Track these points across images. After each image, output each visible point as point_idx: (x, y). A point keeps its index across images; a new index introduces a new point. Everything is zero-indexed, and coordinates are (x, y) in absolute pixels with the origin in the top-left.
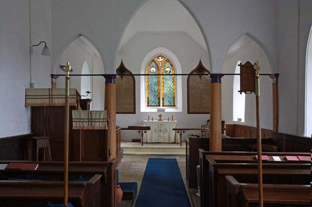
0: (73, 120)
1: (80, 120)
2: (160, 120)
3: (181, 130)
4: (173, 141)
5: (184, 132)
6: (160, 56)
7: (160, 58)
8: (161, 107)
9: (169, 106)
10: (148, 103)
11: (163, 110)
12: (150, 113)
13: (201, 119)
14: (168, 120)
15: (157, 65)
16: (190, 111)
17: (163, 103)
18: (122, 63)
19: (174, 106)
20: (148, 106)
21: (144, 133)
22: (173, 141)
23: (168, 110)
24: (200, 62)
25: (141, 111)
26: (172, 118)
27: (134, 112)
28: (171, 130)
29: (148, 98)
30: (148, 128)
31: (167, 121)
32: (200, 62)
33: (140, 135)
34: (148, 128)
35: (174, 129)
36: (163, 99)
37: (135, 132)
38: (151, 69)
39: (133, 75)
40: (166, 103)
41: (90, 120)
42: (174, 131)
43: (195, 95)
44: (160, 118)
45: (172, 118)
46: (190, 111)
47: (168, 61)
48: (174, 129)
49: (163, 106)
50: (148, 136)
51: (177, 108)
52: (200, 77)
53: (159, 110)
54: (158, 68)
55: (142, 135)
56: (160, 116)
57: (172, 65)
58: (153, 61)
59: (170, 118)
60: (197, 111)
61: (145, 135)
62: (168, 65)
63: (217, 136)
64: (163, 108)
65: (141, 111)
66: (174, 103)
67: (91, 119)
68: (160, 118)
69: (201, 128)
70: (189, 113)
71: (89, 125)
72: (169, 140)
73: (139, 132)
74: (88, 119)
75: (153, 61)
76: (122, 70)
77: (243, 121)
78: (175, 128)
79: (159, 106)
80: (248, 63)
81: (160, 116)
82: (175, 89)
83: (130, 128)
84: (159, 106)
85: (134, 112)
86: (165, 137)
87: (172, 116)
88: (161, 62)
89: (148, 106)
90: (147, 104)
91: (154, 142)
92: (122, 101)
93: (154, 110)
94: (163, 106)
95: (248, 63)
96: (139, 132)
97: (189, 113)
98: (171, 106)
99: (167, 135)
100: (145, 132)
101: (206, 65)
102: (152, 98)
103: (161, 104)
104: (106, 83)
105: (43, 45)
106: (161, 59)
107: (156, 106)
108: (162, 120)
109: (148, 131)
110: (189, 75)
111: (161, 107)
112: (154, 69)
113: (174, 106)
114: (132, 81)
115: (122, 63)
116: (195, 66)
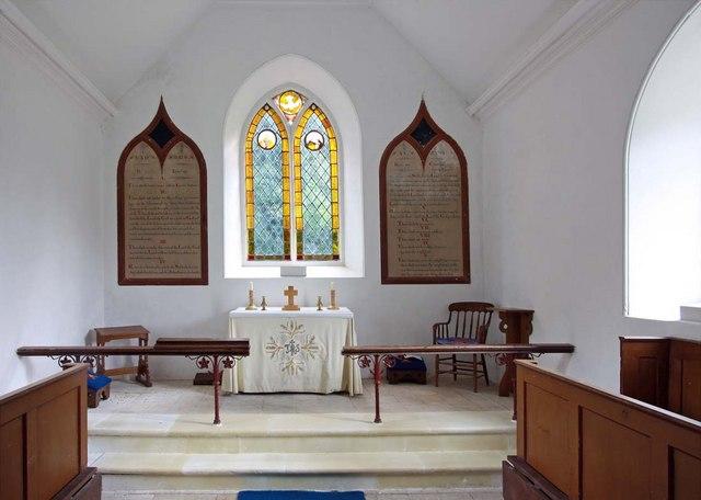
2: (291, 306)
4: (339, 388)
7: (289, 98)
9: (318, 258)
11: (301, 273)
13: (432, 301)
14: (320, 304)
15: (280, 123)
17: (300, 248)
18: (162, 108)
19: (336, 257)
20: (251, 258)
21: (221, 365)
22: (336, 384)
23: (316, 270)
24: (423, 107)
25: (226, 276)
26: (333, 297)
27: (204, 281)
29: (251, 232)
30: (242, 348)
31: (313, 310)
32: (423, 107)
34: (242, 348)
43: (404, 220)
44: (291, 300)
45: (333, 297)
47: (314, 108)
50: (242, 372)
52: (424, 156)
53: (285, 273)
54: (283, 131)
56: (291, 292)
57: (327, 124)
58: (267, 108)
59: (327, 298)
62: (316, 121)
64: (302, 263)
65: (226, 276)
68: (291, 300)
70: (386, 280)
72: (259, 385)
76: (162, 133)
79: (288, 258)
81: (291, 292)
84: (288, 258)
85: (204, 281)
86: (306, 372)
87: (332, 294)
89: (251, 258)
91: (270, 391)
92: (163, 242)
93: (270, 271)
97: (386, 280)
98: (326, 258)
99: (314, 365)
101: (439, 118)
103: (294, 253)
106: (290, 104)
107: (279, 258)
108: (296, 308)
111: (294, 262)
113: (336, 257)
114: (195, 172)
115: (162, 107)
116: (406, 120)
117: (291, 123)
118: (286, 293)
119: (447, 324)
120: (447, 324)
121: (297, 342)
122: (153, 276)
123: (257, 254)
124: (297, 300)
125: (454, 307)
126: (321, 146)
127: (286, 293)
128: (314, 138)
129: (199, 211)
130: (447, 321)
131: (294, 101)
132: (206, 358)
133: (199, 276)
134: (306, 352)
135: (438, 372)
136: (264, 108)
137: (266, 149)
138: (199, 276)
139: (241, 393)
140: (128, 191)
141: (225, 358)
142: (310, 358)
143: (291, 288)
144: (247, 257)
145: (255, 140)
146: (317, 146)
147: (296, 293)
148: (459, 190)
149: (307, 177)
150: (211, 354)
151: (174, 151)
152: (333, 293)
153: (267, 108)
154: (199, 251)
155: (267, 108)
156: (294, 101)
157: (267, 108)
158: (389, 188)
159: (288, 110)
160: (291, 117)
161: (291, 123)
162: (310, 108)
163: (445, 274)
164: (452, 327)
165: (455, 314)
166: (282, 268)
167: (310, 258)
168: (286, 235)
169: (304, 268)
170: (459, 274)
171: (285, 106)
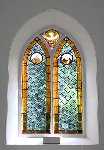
6: (52, 30)
7: (51, 34)
8: (52, 135)
15: (45, 48)
17: (57, 126)
19: (80, 132)
20: (24, 132)
29: (25, 117)
36: (57, 120)
38: (33, 57)
40: (65, 127)
47: (67, 40)
49: (56, 132)
51: (85, 137)
54: (47, 54)
57: (75, 49)
62: (68, 47)
64: (57, 136)
66: (80, 125)
75: (37, 40)
79: (49, 132)
82: (82, 97)
84: (49, 132)
89: (24, 132)
90: (22, 129)
94: (56, 132)
102: (33, 118)
103: (53, 128)
106: (52, 37)
107: (42, 132)
112: (40, 57)
113: (80, 132)
117: (52, 48)
123: (28, 129)
126: (71, 62)
128: (67, 57)
131: (55, 36)
136: (35, 40)
137: (36, 64)
144: (21, 132)
145: (29, 58)
146: (68, 62)
149: (62, 81)
153: (37, 40)
155: (37, 40)
156: (55, 36)
157: (37, 40)
159: (51, 41)
162: (65, 39)
166: (45, 139)
167: (64, 132)
168: (48, 117)
169: (59, 138)
171: (48, 39)
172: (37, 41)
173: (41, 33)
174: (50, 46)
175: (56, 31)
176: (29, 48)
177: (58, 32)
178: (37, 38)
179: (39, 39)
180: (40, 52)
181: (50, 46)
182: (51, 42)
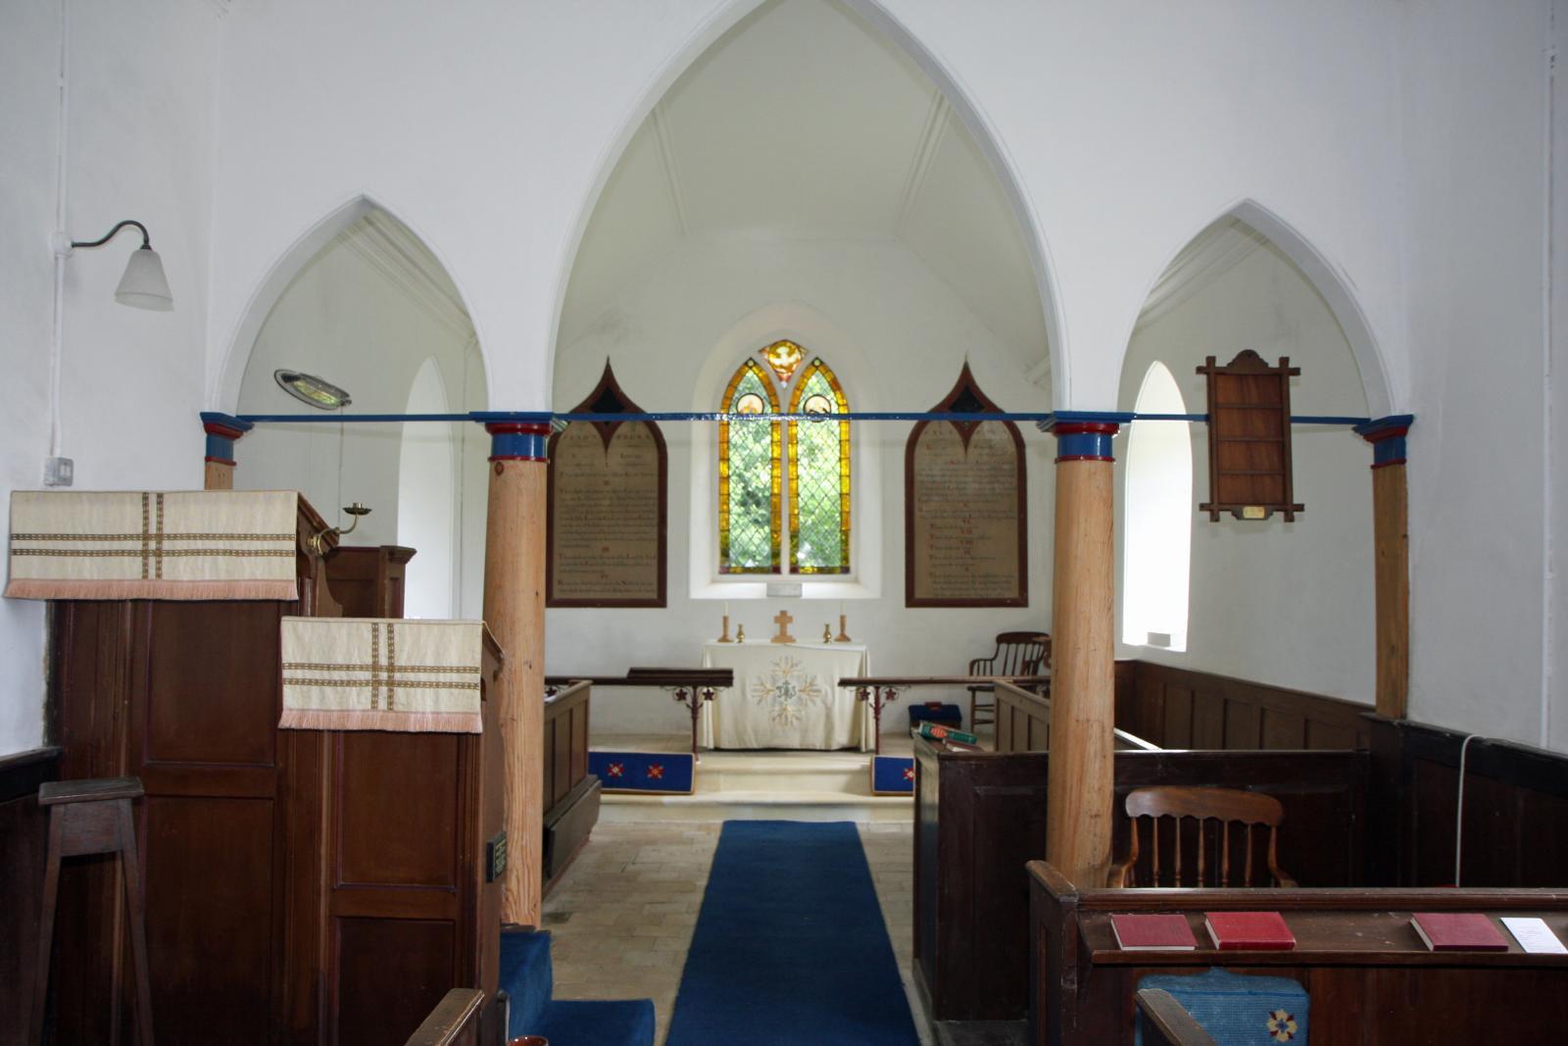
0: (286, 674)
1: (327, 673)
3: (877, 683)
5: (891, 696)
6: (784, 342)
7: (782, 350)
10: (725, 553)
12: (732, 601)
15: (768, 385)
16: (919, 594)
19: (845, 570)
20: (726, 570)
21: (701, 699)
22: (841, 738)
23: (815, 589)
24: (966, 374)
27: (660, 602)
28: (827, 685)
30: (724, 678)
32: (966, 374)
33: (682, 710)
34: (724, 678)
35: (844, 683)
37: (663, 696)
39: (650, 422)
41: (386, 676)
42: (850, 693)
46: (919, 594)
47: (818, 365)
48: (844, 683)
51: (856, 581)
52: (966, 434)
53: (772, 594)
55: (695, 710)
56: (783, 619)
57: (835, 386)
59: (835, 632)
60: (947, 594)
61: (707, 707)
62: (816, 382)
63: (1093, 747)
66: (846, 559)
67: (391, 668)
69: (966, 675)
70: (912, 601)
71: (374, 703)
73: (681, 696)
74: (375, 667)
77: (1179, 644)
78: (854, 675)
79: (776, 570)
80: (1248, 356)
81: (783, 619)
83: (639, 677)
84: (776, 570)
85: (660, 602)
88: (789, 368)
91: (755, 746)
92: (606, 549)
93: (752, 589)
95: (1248, 356)
96: (681, 696)
97: (912, 601)
99: (816, 710)
100: (709, 696)
101: (989, 386)
104: (497, 458)
105: (131, 239)
106: (784, 358)
109: (724, 693)
110: (923, 420)
113: (845, 570)
114: (651, 456)
117: (784, 384)
118: (777, 620)
119: (992, 660)
120: (992, 660)
121: (793, 683)
122: (592, 596)
124: (791, 630)
125: (1004, 639)
127: (777, 620)
129: (656, 509)
130: (992, 656)
131: (790, 354)
132: (685, 690)
133: (654, 596)
134: (804, 696)
135: (974, 722)
136: (746, 364)
138: (654, 596)
139: (717, 750)
140: (559, 483)
141: (705, 690)
142: (809, 703)
143: (783, 613)
144: (717, 569)
147: (790, 619)
148: (1015, 481)
150: (689, 684)
151: (624, 429)
152: (842, 618)
154: (655, 562)
156: (790, 354)
158: (918, 479)
159: (782, 367)
160: (785, 376)
161: (784, 384)
162: (813, 363)
163: (994, 595)
164: (998, 664)
165: (1004, 646)
166: (769, 587)
170: (1014, 594)
171: (773, 359)
172: (751, 368)
173: (760, 348)
174: (781, 379)
175: (794, 344)
176: (732, 385)
177: (798, 347)
178: (751, 359)
179: (755, 363)
180: (757, 392)
181: (781, 379)
182: (783, 370)
